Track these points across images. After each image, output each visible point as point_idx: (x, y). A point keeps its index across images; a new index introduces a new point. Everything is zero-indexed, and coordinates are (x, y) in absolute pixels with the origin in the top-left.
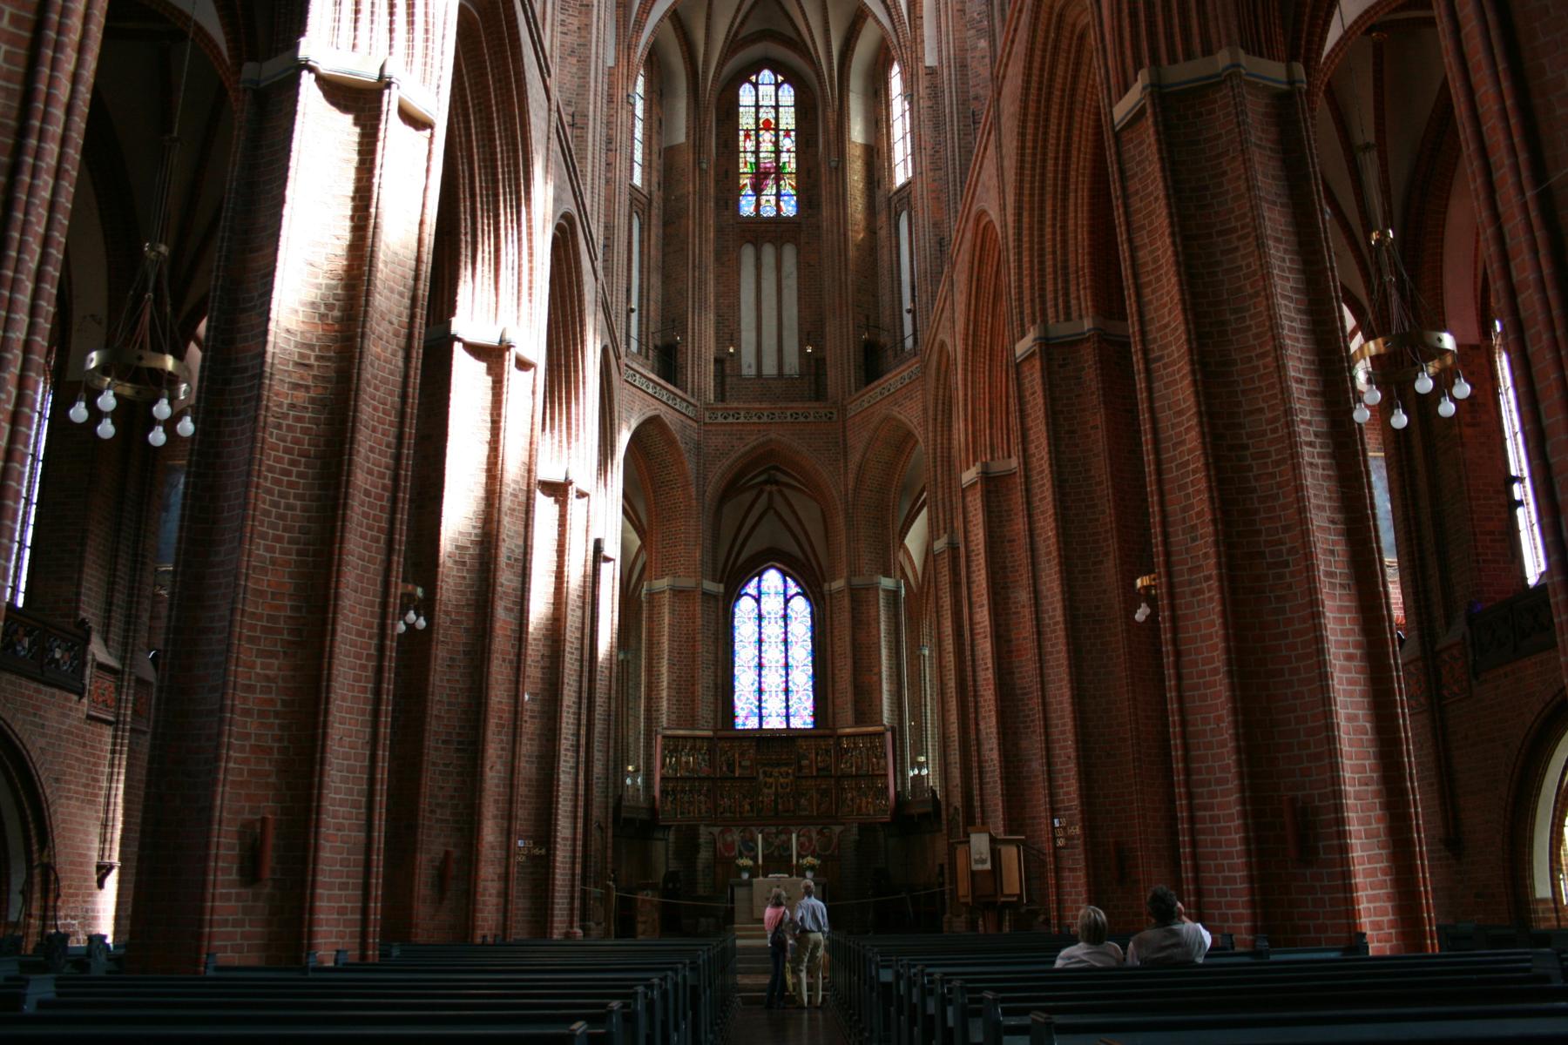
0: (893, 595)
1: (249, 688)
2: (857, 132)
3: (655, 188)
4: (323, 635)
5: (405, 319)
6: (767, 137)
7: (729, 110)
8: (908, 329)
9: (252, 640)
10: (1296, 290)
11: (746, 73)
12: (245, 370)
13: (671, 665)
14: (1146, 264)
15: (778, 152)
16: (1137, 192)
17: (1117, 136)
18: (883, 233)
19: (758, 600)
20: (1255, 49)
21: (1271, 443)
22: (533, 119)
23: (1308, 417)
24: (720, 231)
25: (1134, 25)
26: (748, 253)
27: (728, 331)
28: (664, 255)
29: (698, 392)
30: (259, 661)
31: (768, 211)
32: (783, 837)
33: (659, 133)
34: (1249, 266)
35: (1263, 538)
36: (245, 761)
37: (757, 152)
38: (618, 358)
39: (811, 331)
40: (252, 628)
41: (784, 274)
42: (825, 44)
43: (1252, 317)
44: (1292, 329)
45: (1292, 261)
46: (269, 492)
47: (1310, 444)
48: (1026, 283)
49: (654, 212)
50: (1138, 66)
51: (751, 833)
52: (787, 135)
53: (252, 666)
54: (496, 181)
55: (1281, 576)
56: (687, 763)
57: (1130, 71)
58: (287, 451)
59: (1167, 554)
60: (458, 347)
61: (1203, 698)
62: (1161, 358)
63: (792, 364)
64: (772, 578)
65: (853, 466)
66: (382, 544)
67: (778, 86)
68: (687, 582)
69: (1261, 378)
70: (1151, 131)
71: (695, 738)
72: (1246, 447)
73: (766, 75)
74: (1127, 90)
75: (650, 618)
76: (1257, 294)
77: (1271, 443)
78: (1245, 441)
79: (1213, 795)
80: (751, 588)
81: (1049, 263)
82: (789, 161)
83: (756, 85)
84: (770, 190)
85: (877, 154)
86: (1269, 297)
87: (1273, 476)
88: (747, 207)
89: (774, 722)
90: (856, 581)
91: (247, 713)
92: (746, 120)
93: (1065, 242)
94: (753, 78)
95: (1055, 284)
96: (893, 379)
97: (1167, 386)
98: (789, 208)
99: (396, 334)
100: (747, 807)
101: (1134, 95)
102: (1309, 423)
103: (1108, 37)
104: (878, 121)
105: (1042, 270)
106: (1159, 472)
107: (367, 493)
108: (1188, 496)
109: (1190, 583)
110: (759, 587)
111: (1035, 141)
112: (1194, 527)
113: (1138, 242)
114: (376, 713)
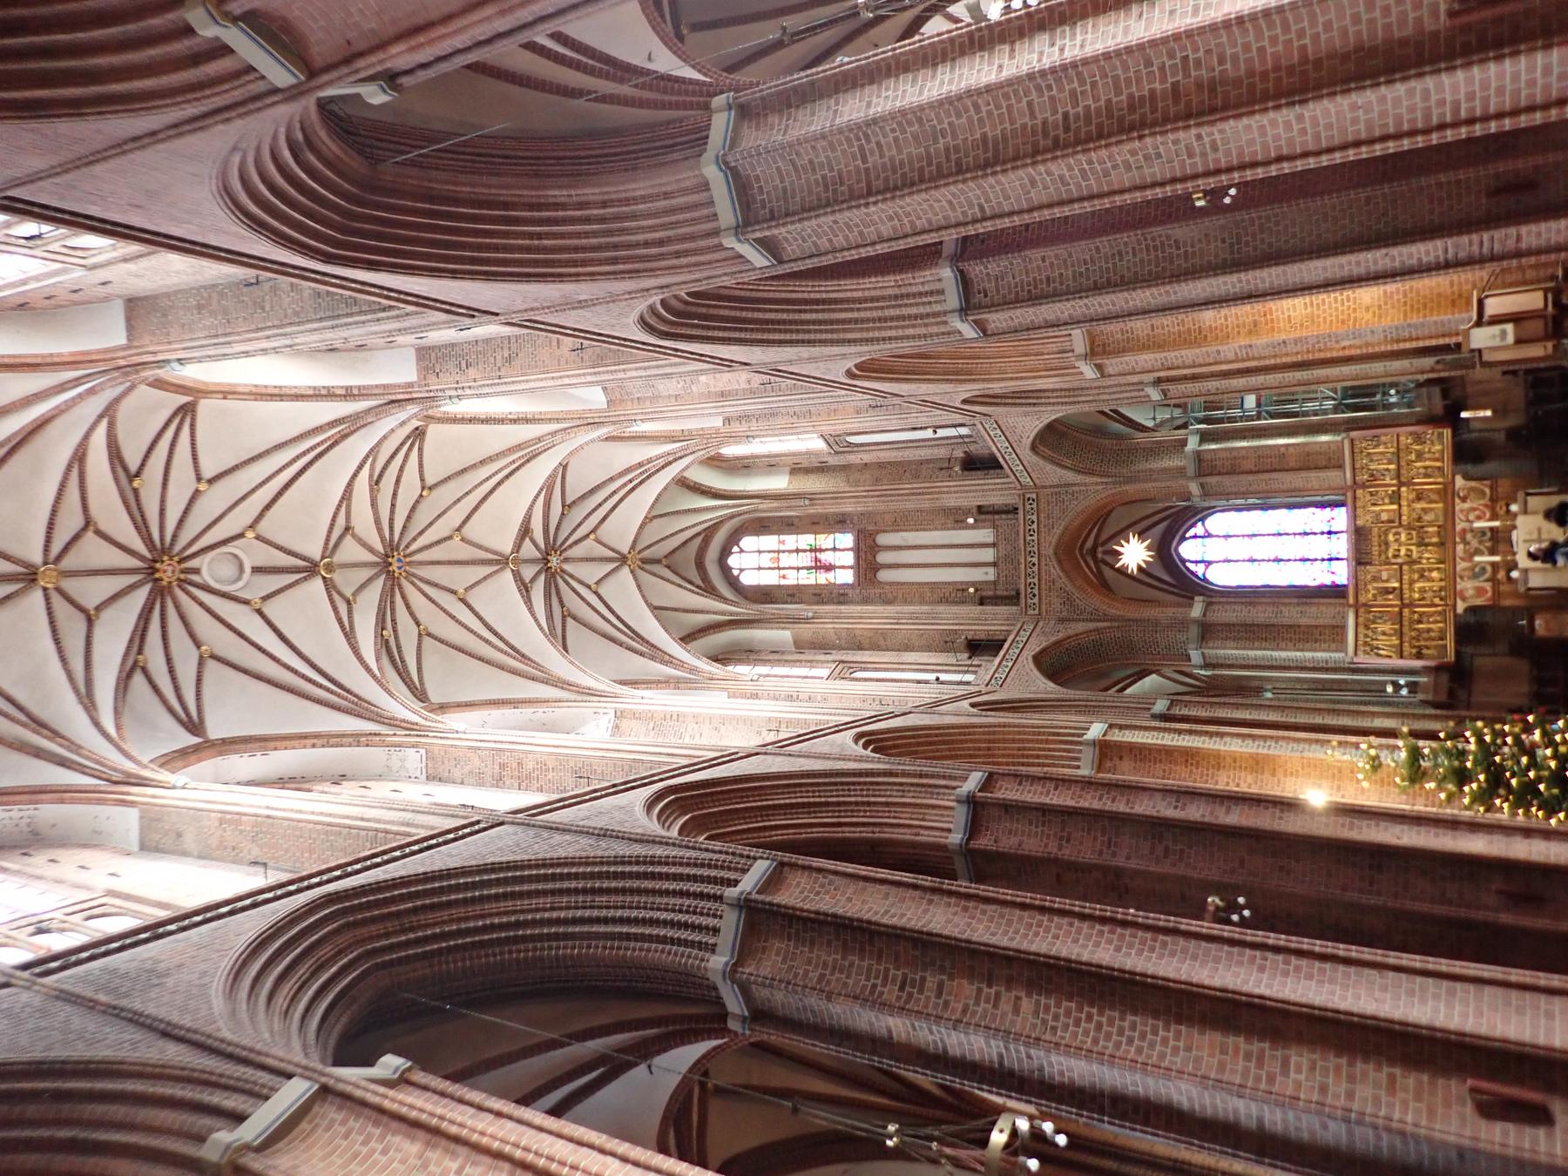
0: (1205, 437)
1: (1323, 1089)
2: (779, 483)
3: (830, 658)
4: (1263, 1009)
5: (953, 900)
6: (786, 560)
7: (765, 595)
8: (951, 432)
9: (1271, 1079)
10: (914, 81)
11: (733, 583)
12: (1001, 1056)
13: (1278, 649)
14: (894, 229)
15: (797, 551)
16: (830, 241)
17: (781, 262)
18: (867, 458)
19: (1208, 563)
20: (698, 139)
21: (1061, 90)
22: (774, 770)
23: (1035, 56)
24: (866, 601)
25: (686, 253)
26: (884, 575)
27: (955, 594)
28: (888, 650)
29: (1010, 620)
30: (1292, 1075)
31: (849, 558)
32: (1469, 536)
33: (783, 653)
34: (893, 131)
35: (1157, 86)
36: (1405, 1103)
37: (798, 569)
38: (980, 693)
39: (955, 518)
40: (1258, 1079)
41: (903, 544)
42: (708, 511)
43: (940, 122)
44: (951, 82)
45: (887, 89)
46: (1118, 1045)
47: (1062, 50)
48: (911, 331)
49: (850, 658)
50: (719, 247)
52: (783, 542)
53: (1298, 1084)
54: (827, 804)
55: (1198, 63)
57: (723, 254)
58: (1077, 1023)
59: (1174, 180)
60: (974, 844)
61: (1329, 126)
62: (981, 208)
63: (985, 535)
64: (1188, 550)
65: (1079, 478)
66: (1168, 939)
67: (742, 551)
68: (1194, 631)
69: (998, 107)
70: (775, 232)
72: (1066, 116)
73: (734, 561)
74: (741, 256)
75: (1230, 666)
76: (920, 120)
77: (1061, 90)
78: (1060, 116)
79: (1441, 103)
80: (1199, 569)
81: (892, 312)
82: (806, 540)
83: (741, 570)
84: (826, 557)
85: (800, 467)
86: (921, 108)
87: (1094, 84)
88: (846, 577)
90: (1191, 471)
91: (1350, 1095)
92: (770, 579)
93: (872, 300)
94: (736, 573)
95: (911, 305)
96: (997, 446)
97: (1007, 198)
98: (846, 540)
99: (965, 909)
100: (1435, 574)
101: (746, 250)
102: (1041, 53)
103: (697, 276)
104: (770, 464)
105: (898, 318)
106: (1091, 197)
107: (1118, 949)
108: (1115, 167)
109: (1204, 154)
110: (1196, 562)
111: (786, 331)
112: (1146, 157)
113: (874, 237)
114: (1347, 961)
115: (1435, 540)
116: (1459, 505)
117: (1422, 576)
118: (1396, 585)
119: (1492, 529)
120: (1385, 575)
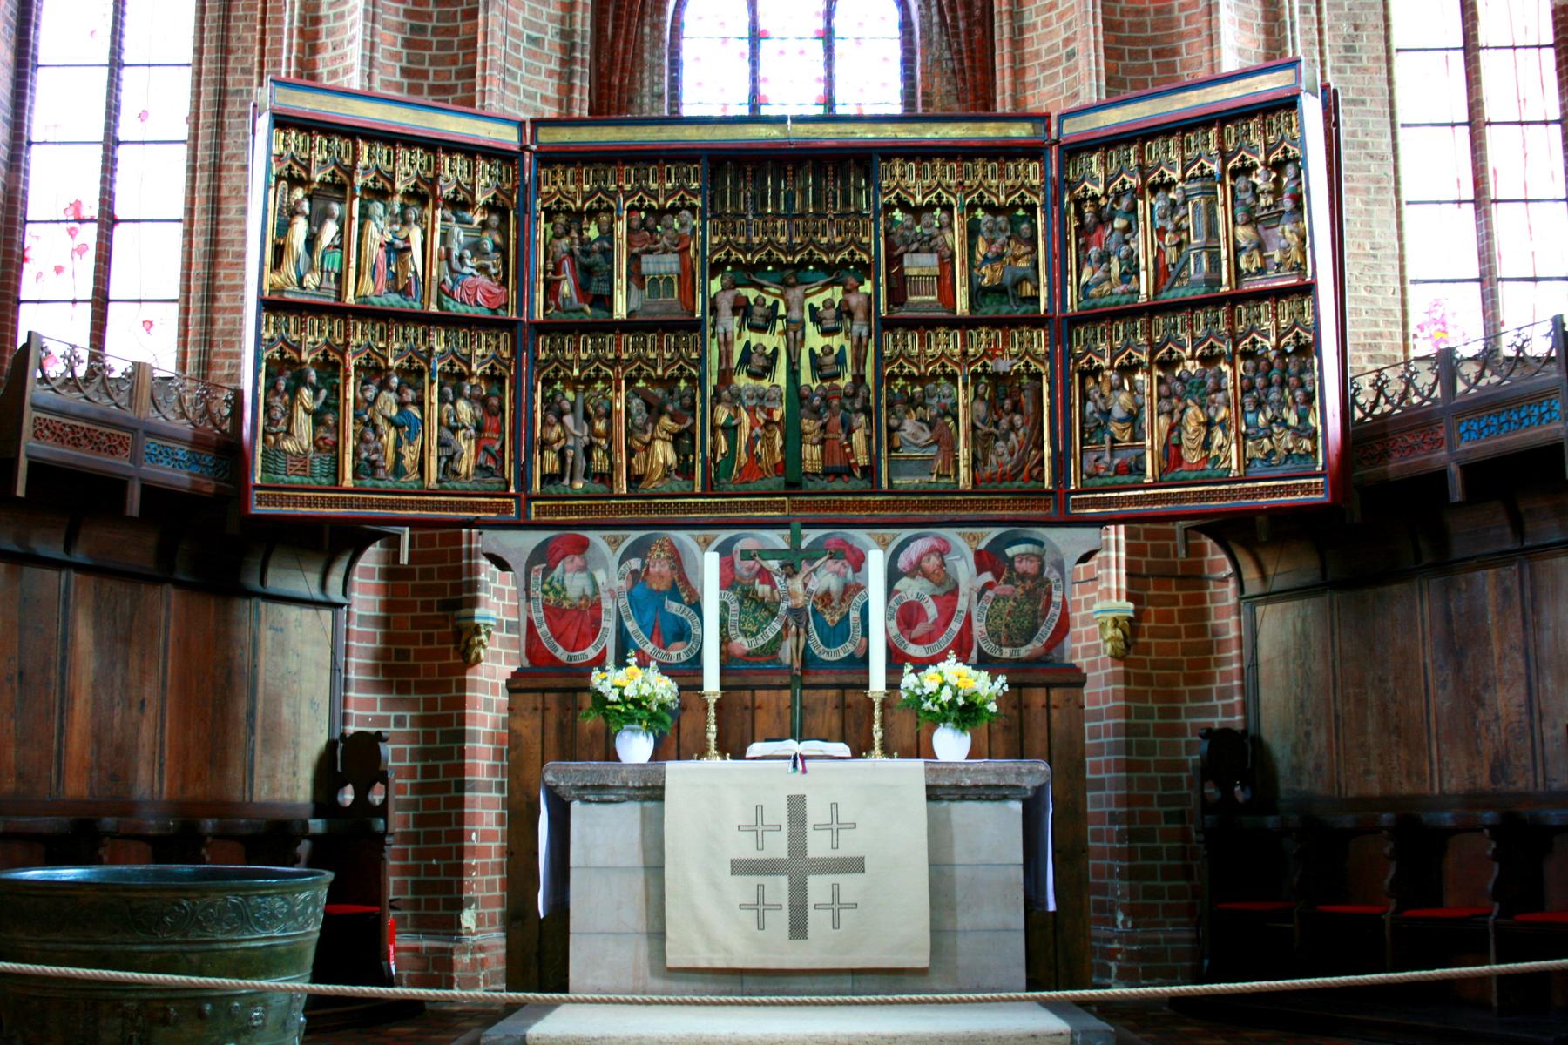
32: (826, 578)
51: (676, 557)
56: (396, 251)
71: (433, 146)
89: (792, 93)
100: (664, 453)
115: (812, 454)
116: (962, 547)
117: (655, 410)
118: (620, 310)
119: (861, 662)
120: (662, 264)
